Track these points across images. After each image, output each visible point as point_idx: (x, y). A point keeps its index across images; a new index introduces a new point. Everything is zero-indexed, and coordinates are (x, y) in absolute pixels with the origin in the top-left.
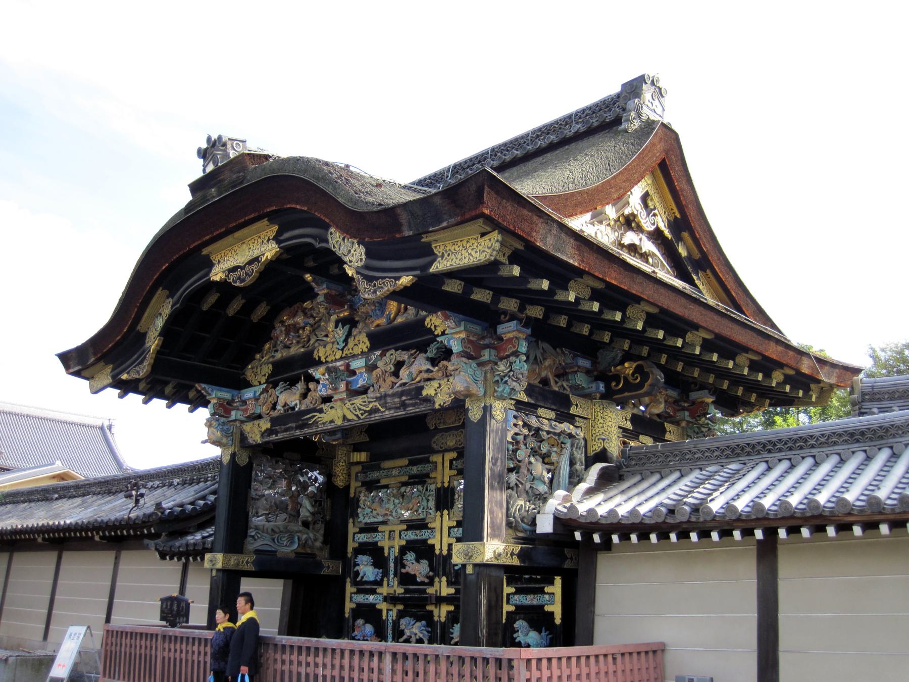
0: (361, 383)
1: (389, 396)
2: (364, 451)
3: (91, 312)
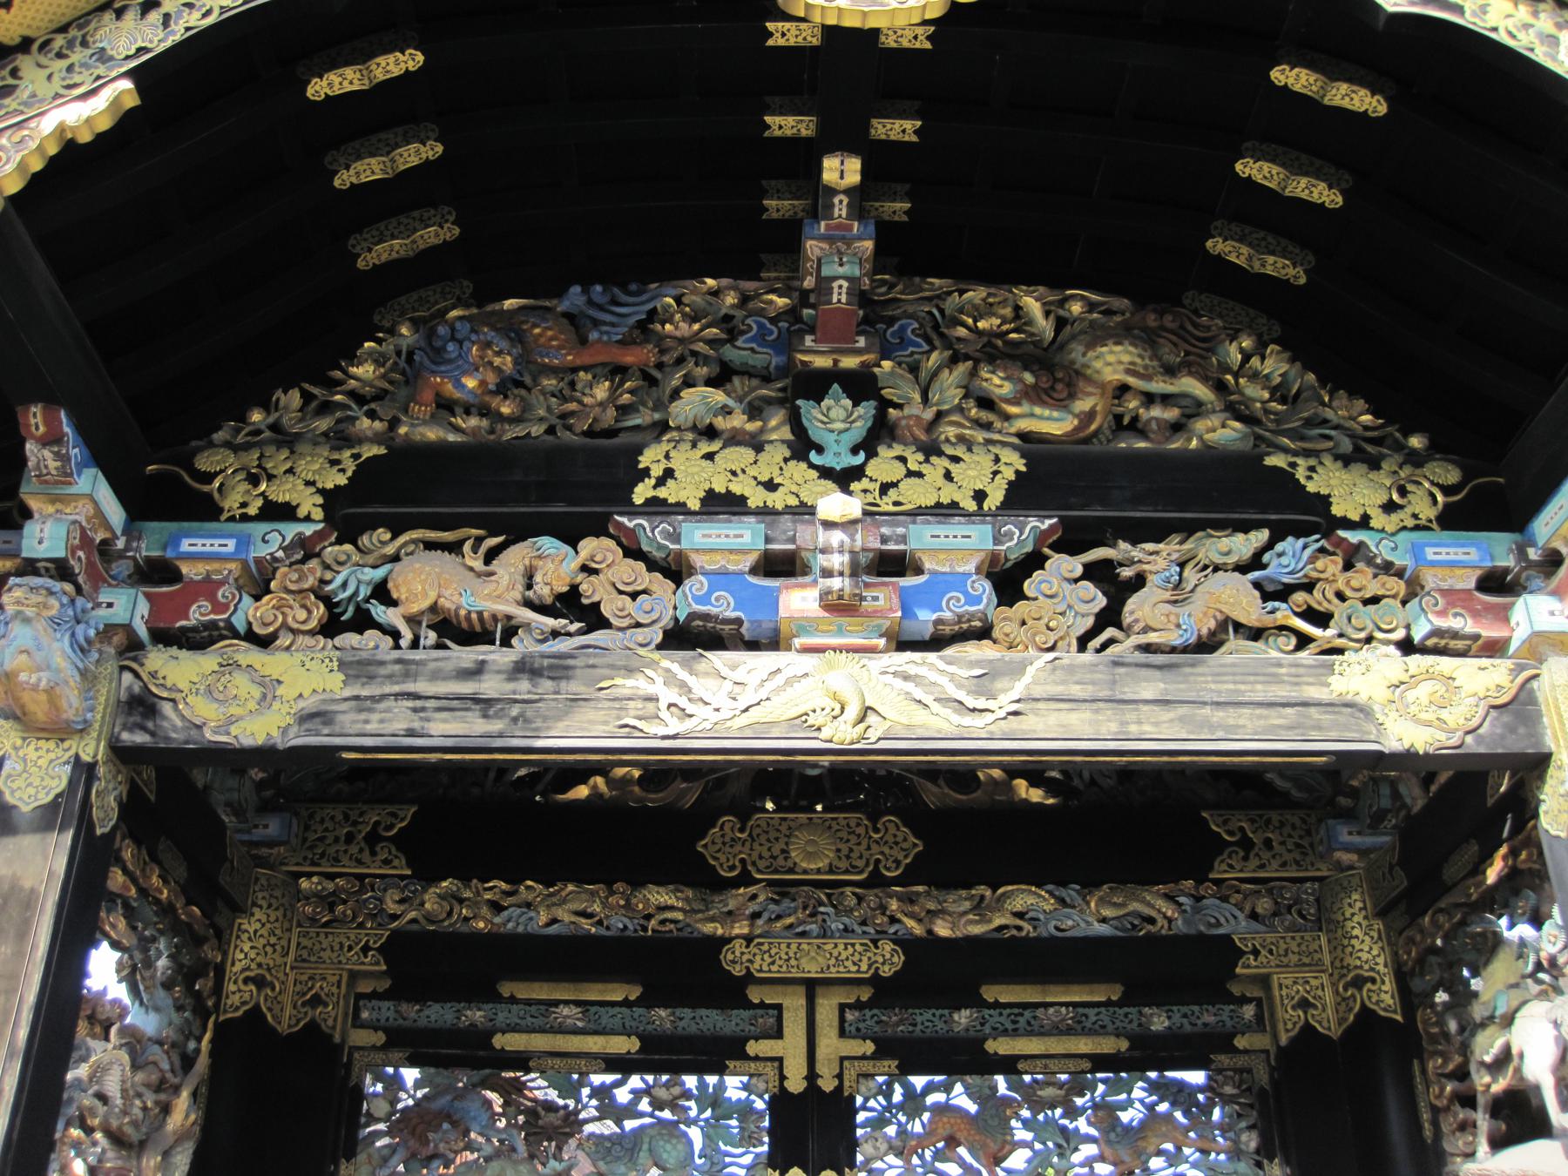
0: (952, 608)
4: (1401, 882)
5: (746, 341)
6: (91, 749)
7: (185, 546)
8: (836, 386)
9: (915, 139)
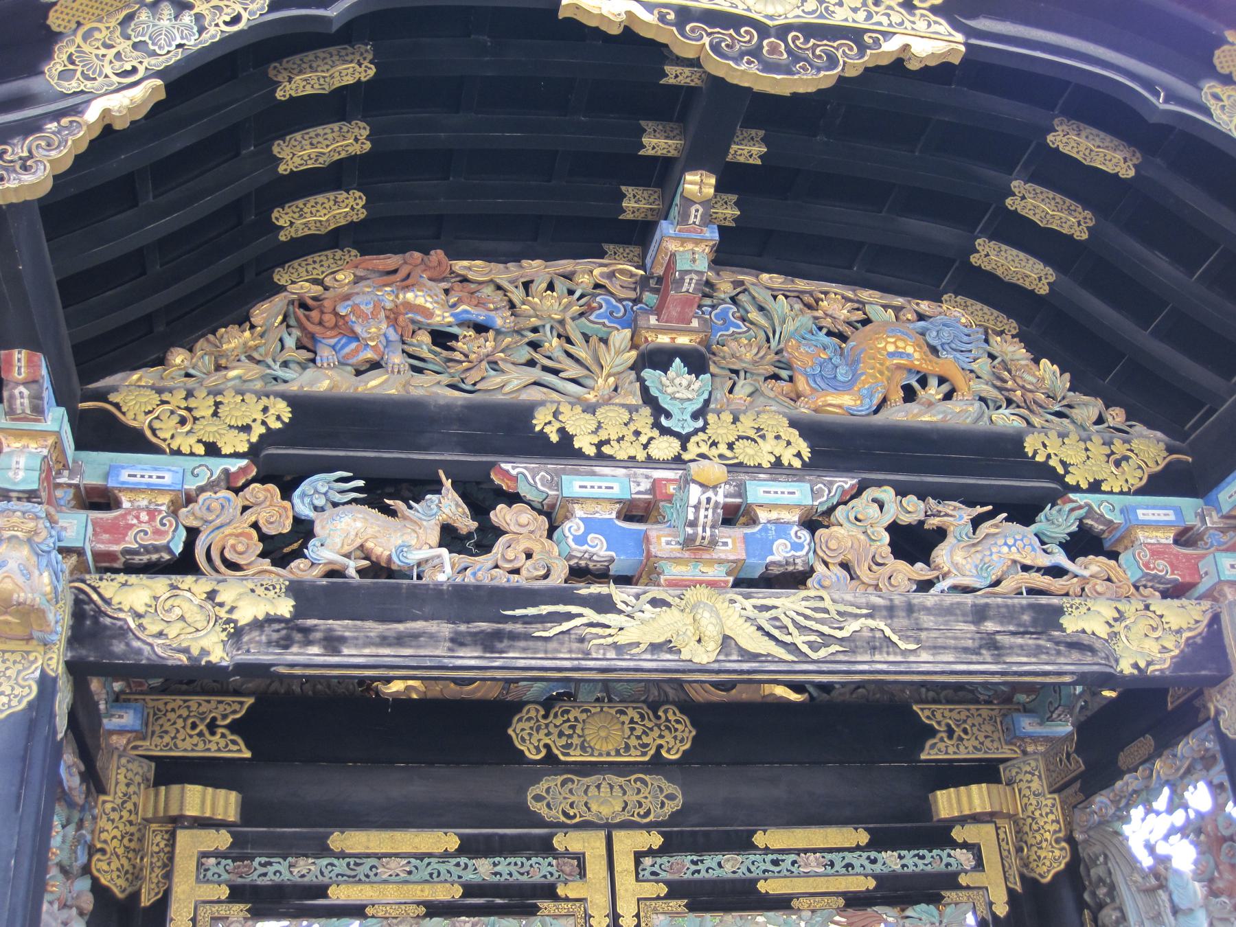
0: (780, 552)
1: (928, 610)
2: (230, 787)
4: (1078, 765)
5: (598, 316)
6: (55, 662)
7: (124, 476)
8: (678, 360)
9: (759, 162)
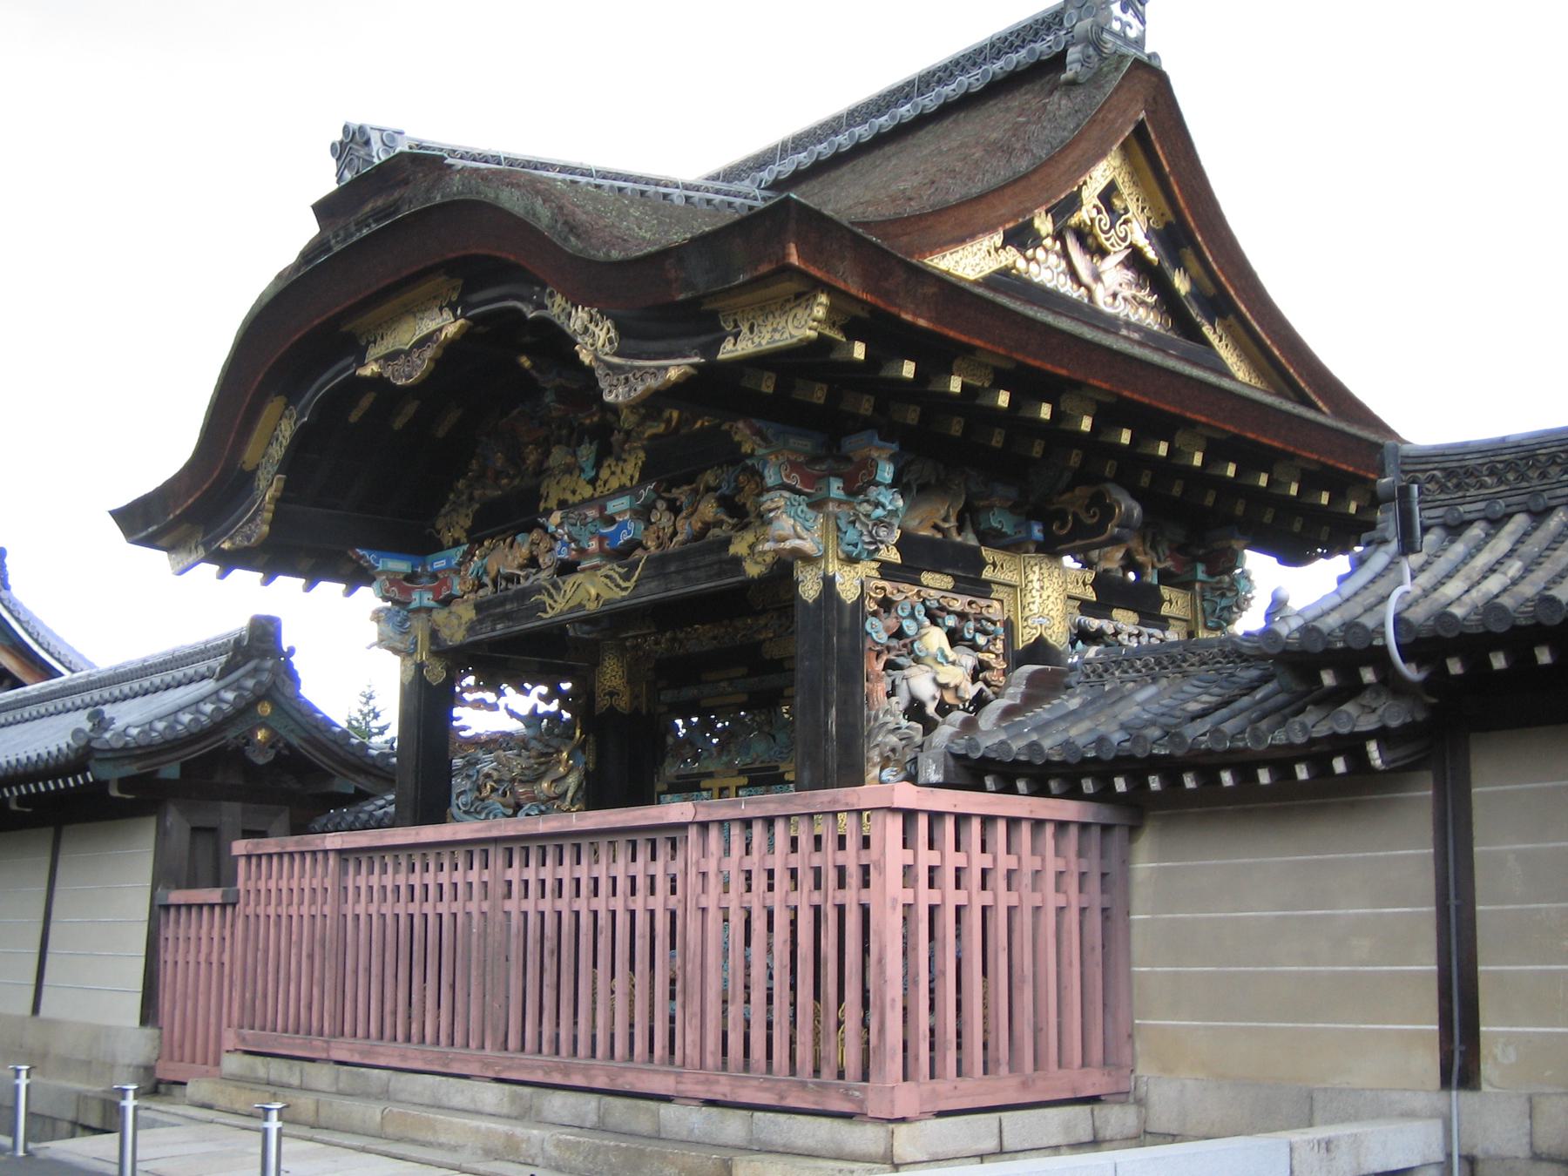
0: (624, 537)
3: (166, 445)
